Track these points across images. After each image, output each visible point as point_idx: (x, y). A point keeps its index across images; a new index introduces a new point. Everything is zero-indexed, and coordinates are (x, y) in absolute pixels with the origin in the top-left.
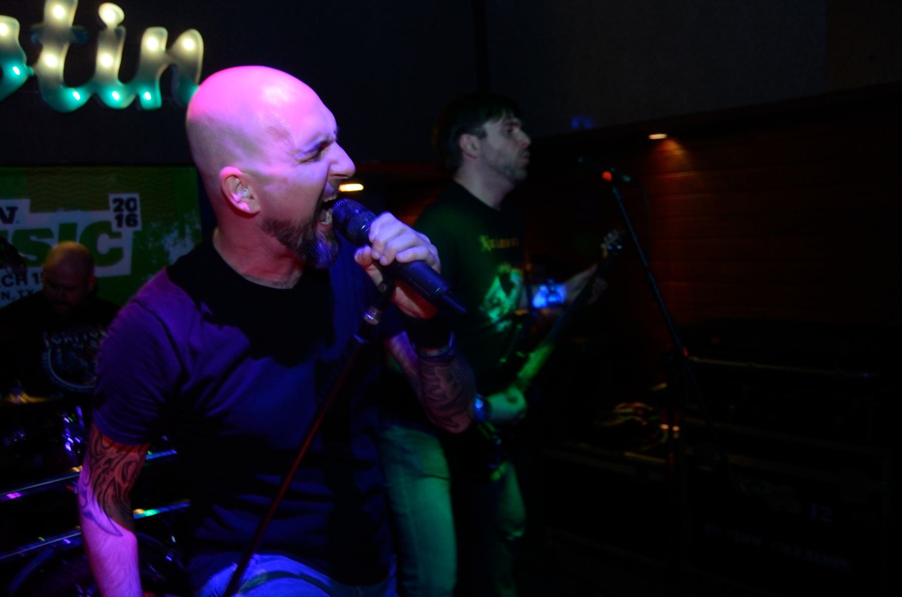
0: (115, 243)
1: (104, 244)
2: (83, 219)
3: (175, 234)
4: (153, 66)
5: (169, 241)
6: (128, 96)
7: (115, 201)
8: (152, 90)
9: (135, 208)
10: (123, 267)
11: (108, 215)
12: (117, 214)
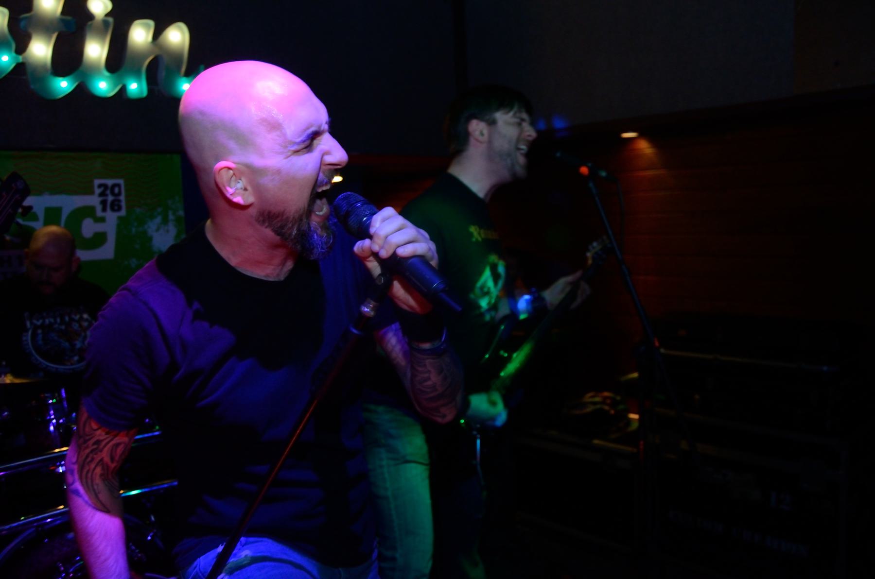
0: (99, 227)
1: (89, 228)
2: (69, 203)
3: (158, 220)
4: (139, 56)
5: (152, 226)
6: (116, 86)
7: (100, 186)
9: (120, 194)
10: (107, 252)
11: (94, 200)
12: (101, 199)
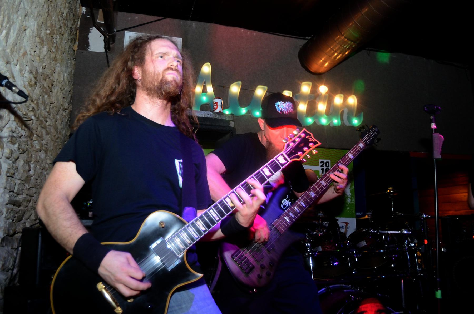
7: (321, 162)
8: (338, 119)
9: (329, 166)
